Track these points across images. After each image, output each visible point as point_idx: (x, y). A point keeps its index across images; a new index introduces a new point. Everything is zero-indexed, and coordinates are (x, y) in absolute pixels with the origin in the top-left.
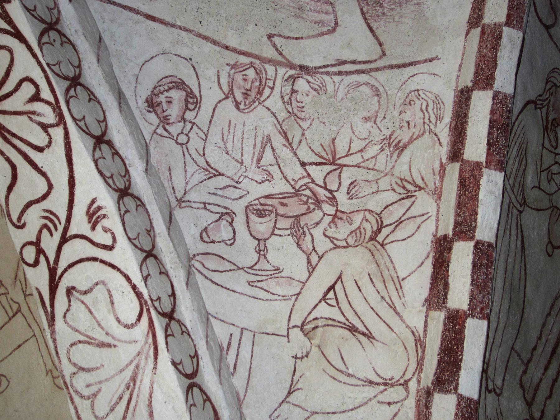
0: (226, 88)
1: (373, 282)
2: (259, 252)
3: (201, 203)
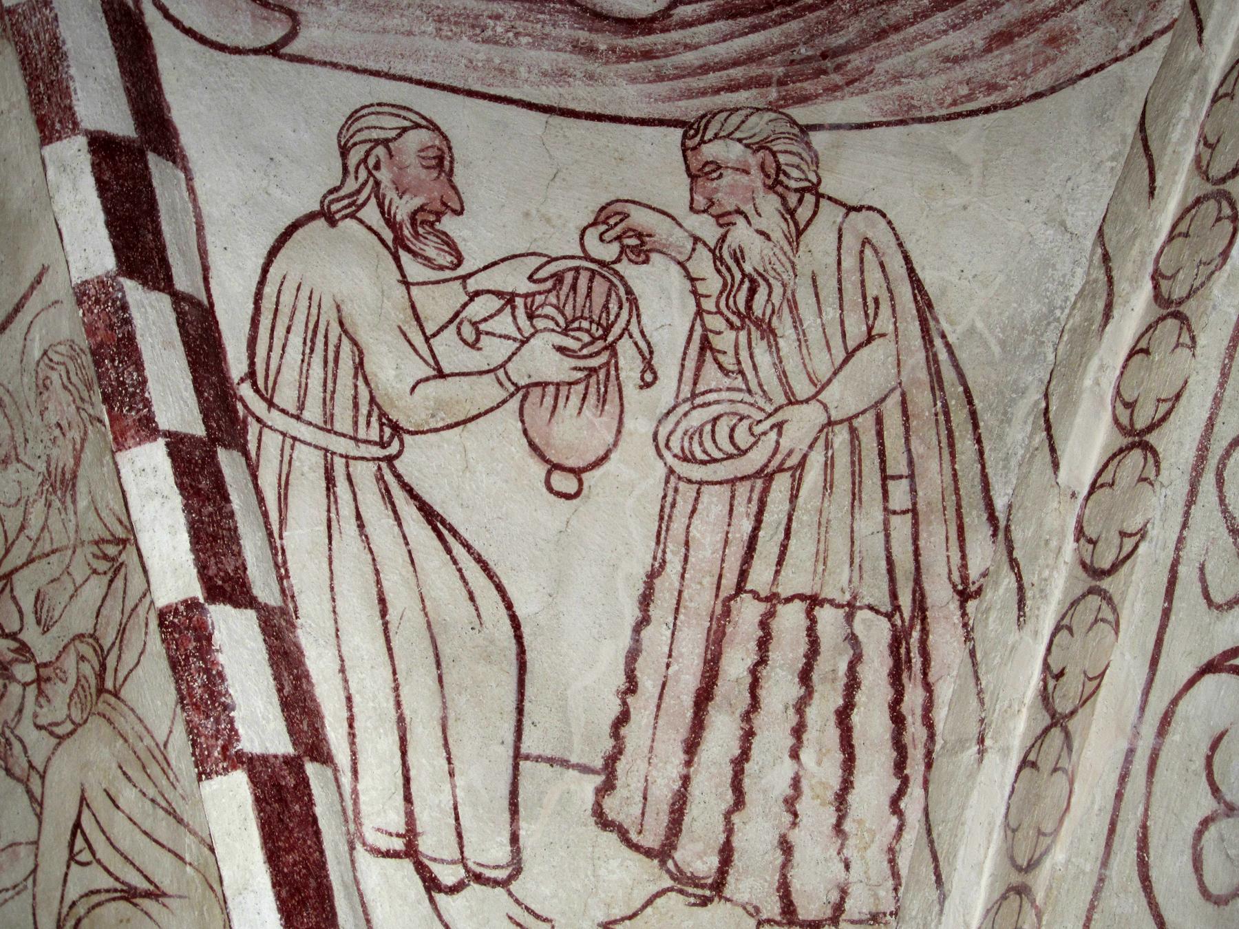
1: (129, 779)
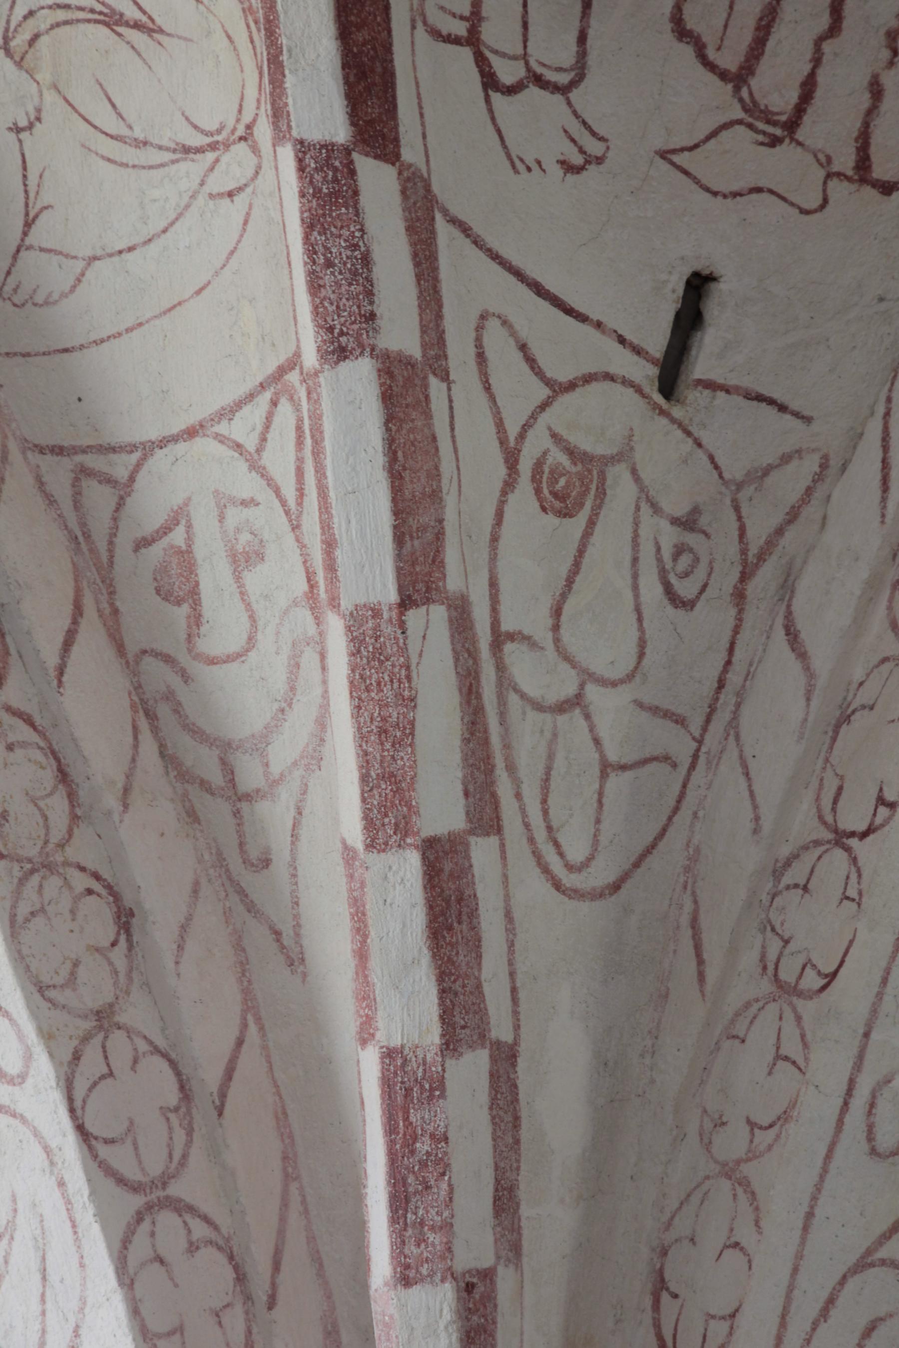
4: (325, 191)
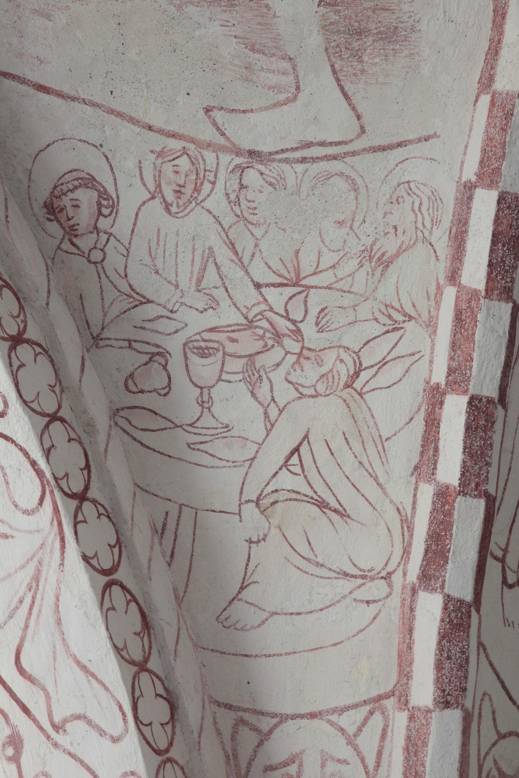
0: (151, 186)
1: (348, 443)
2: (201, 404)
3: (124, 340)
4: (455, 622)
